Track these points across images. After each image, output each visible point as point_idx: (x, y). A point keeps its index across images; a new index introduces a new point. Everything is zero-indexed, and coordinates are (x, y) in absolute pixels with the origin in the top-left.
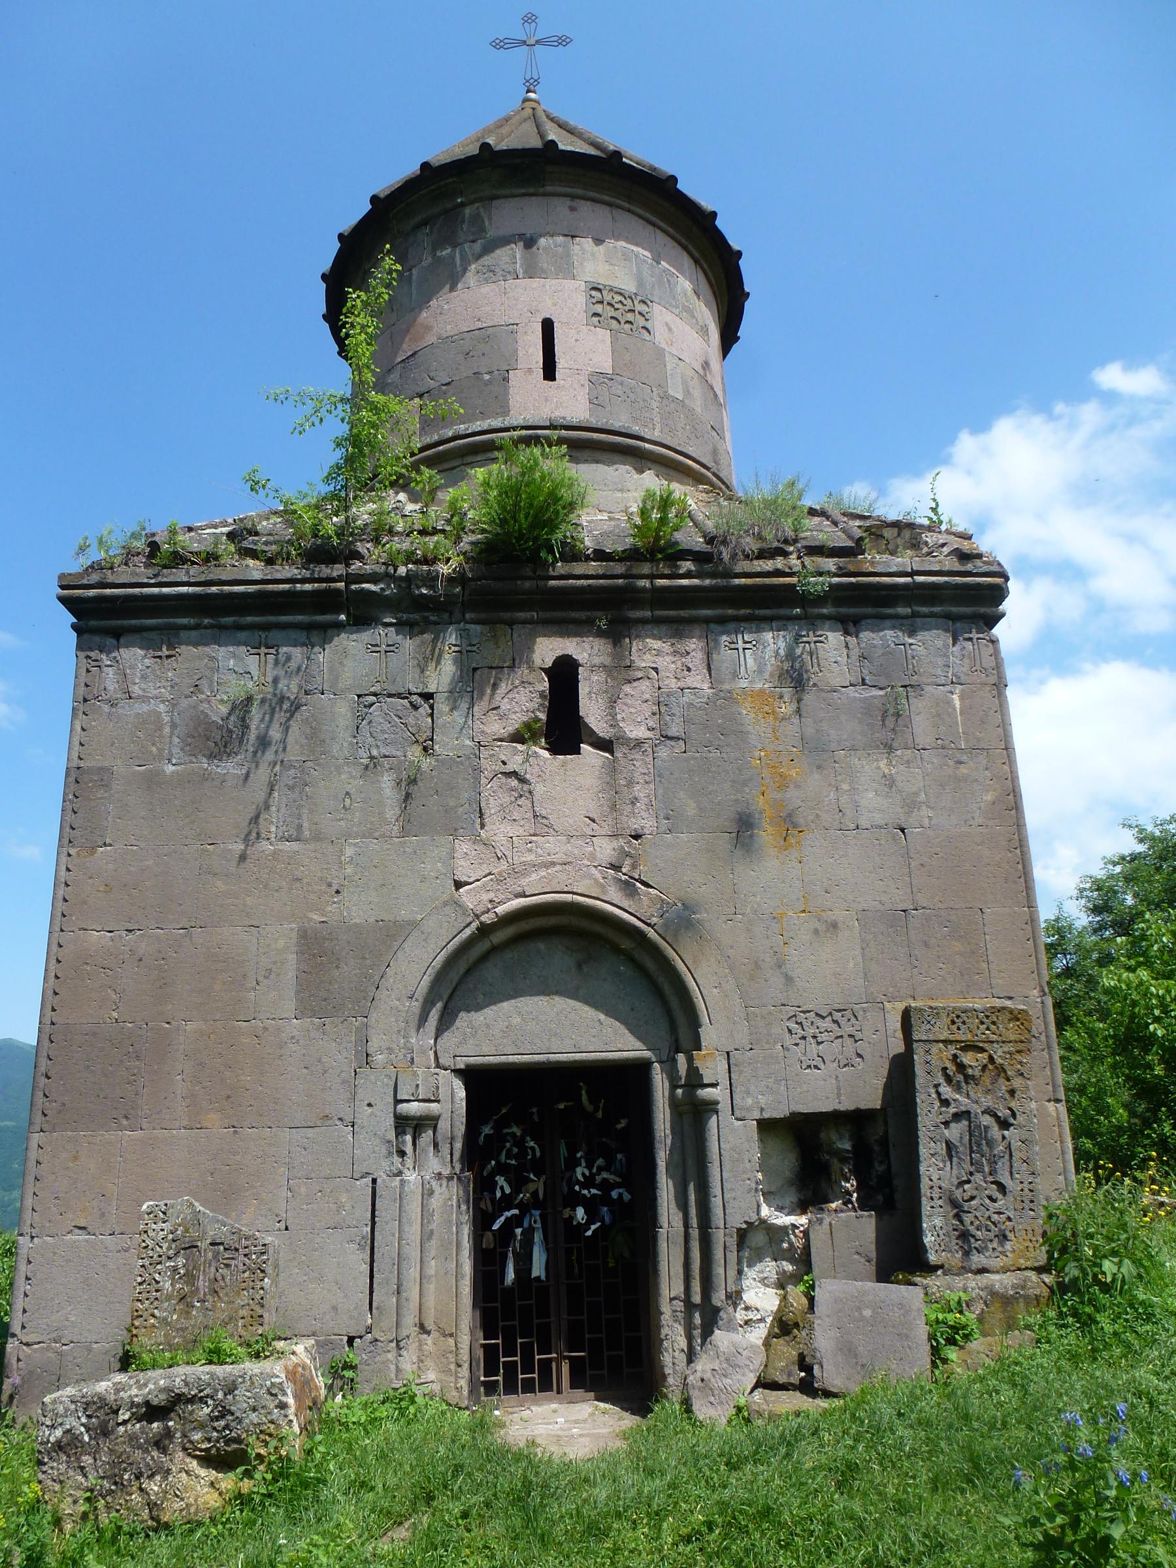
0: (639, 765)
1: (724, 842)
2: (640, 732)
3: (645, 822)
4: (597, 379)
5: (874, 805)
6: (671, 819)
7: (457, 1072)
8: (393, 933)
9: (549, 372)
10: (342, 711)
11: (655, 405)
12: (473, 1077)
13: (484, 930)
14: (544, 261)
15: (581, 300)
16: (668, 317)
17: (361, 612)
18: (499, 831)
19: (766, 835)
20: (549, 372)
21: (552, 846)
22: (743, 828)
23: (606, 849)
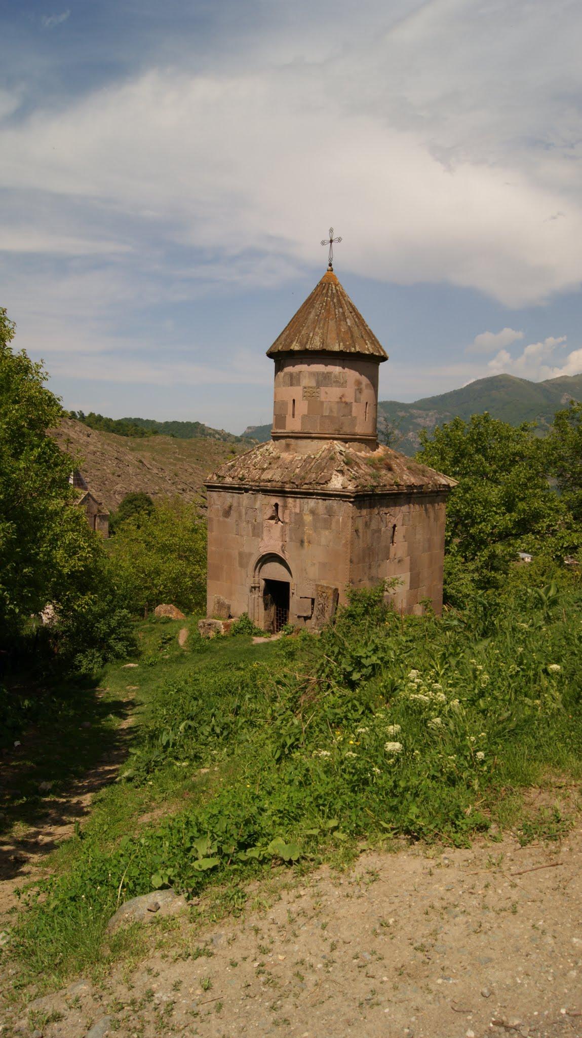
0: (287, 528)
1: (299, 544)
2: (287, 521)
3: (287, 539)
4: (304, 417)
5: (323, 541)
6: (291, 538)
7: (265, 580)
8: (250, 554)
9: (293, 415)
10: (244, 511)
11: (318, 421)
12: (265, 580)
13: (263, 556)
14: (294, 382)
15: (301, 392)
16: (326, 389)
17: (247, 491)
18: (266, 538)
19: (306, 544)
20: (293, 415)
21: (272, 542)
22: (302, 542)
23: (281, 544)
